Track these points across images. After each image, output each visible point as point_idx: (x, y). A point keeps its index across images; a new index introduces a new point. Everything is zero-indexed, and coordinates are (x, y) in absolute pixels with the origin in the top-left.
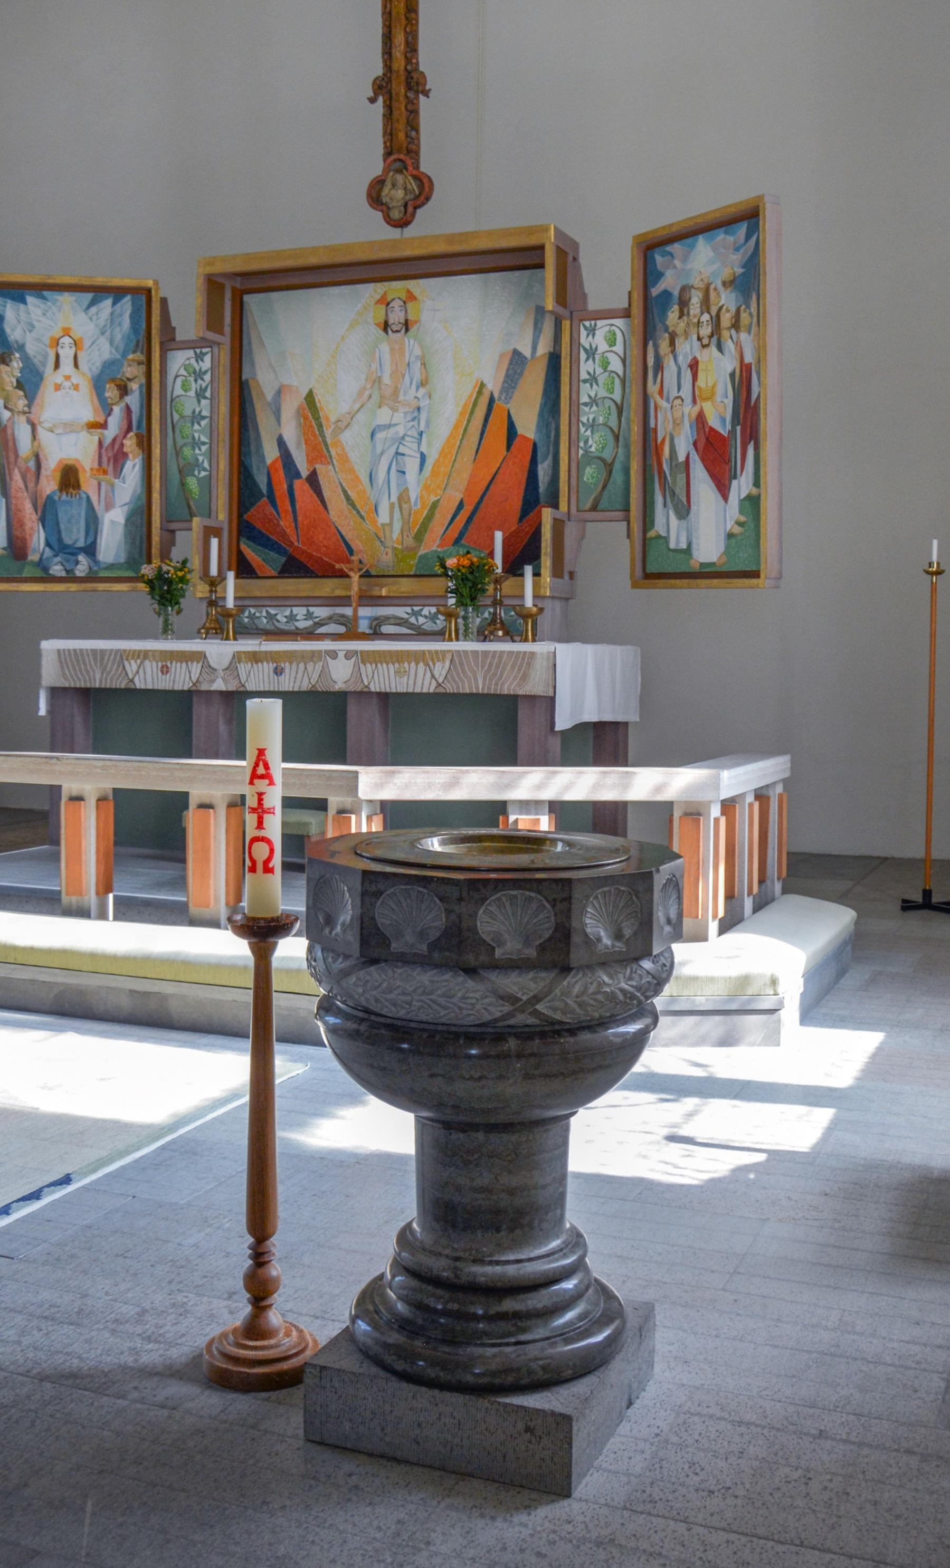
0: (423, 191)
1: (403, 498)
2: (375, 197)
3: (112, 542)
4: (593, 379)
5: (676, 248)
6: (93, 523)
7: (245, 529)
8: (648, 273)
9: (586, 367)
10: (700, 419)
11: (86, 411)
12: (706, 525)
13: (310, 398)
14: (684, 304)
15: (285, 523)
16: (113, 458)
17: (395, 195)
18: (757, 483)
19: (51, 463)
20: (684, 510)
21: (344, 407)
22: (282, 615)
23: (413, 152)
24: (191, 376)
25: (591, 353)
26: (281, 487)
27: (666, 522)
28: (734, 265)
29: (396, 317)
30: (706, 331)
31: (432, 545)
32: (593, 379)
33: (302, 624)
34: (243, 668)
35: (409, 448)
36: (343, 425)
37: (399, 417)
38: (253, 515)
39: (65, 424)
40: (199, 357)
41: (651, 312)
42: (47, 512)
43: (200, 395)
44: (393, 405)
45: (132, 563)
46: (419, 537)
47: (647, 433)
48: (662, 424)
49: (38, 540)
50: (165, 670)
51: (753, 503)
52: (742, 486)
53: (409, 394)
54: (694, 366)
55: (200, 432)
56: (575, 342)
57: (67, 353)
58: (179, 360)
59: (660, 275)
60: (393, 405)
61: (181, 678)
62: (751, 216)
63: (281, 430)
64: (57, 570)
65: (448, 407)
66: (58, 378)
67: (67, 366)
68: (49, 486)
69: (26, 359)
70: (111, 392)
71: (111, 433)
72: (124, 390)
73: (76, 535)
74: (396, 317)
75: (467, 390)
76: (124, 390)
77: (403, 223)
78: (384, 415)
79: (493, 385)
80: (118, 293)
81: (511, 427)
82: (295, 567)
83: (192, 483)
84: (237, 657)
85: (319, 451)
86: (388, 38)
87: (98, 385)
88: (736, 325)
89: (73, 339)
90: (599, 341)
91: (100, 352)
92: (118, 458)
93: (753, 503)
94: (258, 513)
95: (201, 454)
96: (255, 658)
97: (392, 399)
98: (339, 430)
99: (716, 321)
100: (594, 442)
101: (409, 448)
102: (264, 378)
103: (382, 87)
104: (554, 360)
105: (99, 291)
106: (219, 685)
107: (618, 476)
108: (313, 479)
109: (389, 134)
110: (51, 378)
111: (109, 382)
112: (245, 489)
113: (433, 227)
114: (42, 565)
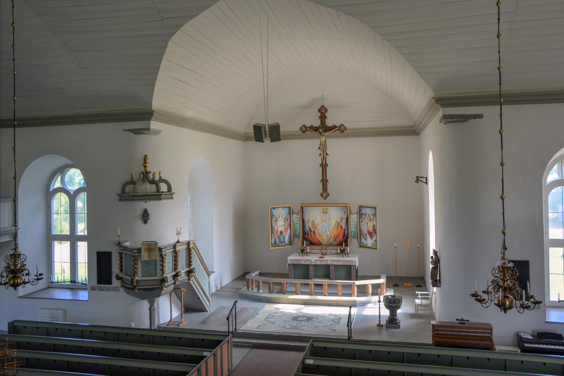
0: (328, 195)
1: (327, 235)
2: (322, 195)
3: (287, 241)
6: (284, 238)
7: (304, 238)
8: (360, 210)
9: (352, 220)
10: (368, 230)
11: (283, 224)
12: (369, 242)
13: (313, 221)
14: (365, 215)
15: (310, 237)
17: (324, 195)
20: (366, 240)
22: (313, 251)
23: (326, 190)
24: (296, 218)
27: (363, 240)
28: (373, 213)
29: (325, 211)
31: (331, 241)
35: (327, 228)
36: (318, 225)
38: (305, 236)
39: (280, 225)
41: (360, 215)
42: (279, 238)
44: (325, 223)
47: (360, 229)
48: (362, 228)
49: (278, 241)
51: (376, 241)
52: (374, 238)
55: (298, 225)
58: (294, 216)
60: (325, 223)
63: (309, 225)
65: (333, 223)
68: (279, 234)
73: (282, 240)
75: (335, 221)
77: (326, 198)
78: (324, 224)
79: (339, 221)
81: (341, 227)
82: (312, 244)
85: (315, 228)
86: (323, 174)
87: (284, 220)
89: (281, 213)
92: (287, 229)
93: (376, 241)
94: (306, 236)
95: (298, 228)
100: (353, 229)
103: (322, 181)
108: (314, 232)
109: (323, 187)
110: (279, 219)
111: (286, 219)
112: (304, 233)
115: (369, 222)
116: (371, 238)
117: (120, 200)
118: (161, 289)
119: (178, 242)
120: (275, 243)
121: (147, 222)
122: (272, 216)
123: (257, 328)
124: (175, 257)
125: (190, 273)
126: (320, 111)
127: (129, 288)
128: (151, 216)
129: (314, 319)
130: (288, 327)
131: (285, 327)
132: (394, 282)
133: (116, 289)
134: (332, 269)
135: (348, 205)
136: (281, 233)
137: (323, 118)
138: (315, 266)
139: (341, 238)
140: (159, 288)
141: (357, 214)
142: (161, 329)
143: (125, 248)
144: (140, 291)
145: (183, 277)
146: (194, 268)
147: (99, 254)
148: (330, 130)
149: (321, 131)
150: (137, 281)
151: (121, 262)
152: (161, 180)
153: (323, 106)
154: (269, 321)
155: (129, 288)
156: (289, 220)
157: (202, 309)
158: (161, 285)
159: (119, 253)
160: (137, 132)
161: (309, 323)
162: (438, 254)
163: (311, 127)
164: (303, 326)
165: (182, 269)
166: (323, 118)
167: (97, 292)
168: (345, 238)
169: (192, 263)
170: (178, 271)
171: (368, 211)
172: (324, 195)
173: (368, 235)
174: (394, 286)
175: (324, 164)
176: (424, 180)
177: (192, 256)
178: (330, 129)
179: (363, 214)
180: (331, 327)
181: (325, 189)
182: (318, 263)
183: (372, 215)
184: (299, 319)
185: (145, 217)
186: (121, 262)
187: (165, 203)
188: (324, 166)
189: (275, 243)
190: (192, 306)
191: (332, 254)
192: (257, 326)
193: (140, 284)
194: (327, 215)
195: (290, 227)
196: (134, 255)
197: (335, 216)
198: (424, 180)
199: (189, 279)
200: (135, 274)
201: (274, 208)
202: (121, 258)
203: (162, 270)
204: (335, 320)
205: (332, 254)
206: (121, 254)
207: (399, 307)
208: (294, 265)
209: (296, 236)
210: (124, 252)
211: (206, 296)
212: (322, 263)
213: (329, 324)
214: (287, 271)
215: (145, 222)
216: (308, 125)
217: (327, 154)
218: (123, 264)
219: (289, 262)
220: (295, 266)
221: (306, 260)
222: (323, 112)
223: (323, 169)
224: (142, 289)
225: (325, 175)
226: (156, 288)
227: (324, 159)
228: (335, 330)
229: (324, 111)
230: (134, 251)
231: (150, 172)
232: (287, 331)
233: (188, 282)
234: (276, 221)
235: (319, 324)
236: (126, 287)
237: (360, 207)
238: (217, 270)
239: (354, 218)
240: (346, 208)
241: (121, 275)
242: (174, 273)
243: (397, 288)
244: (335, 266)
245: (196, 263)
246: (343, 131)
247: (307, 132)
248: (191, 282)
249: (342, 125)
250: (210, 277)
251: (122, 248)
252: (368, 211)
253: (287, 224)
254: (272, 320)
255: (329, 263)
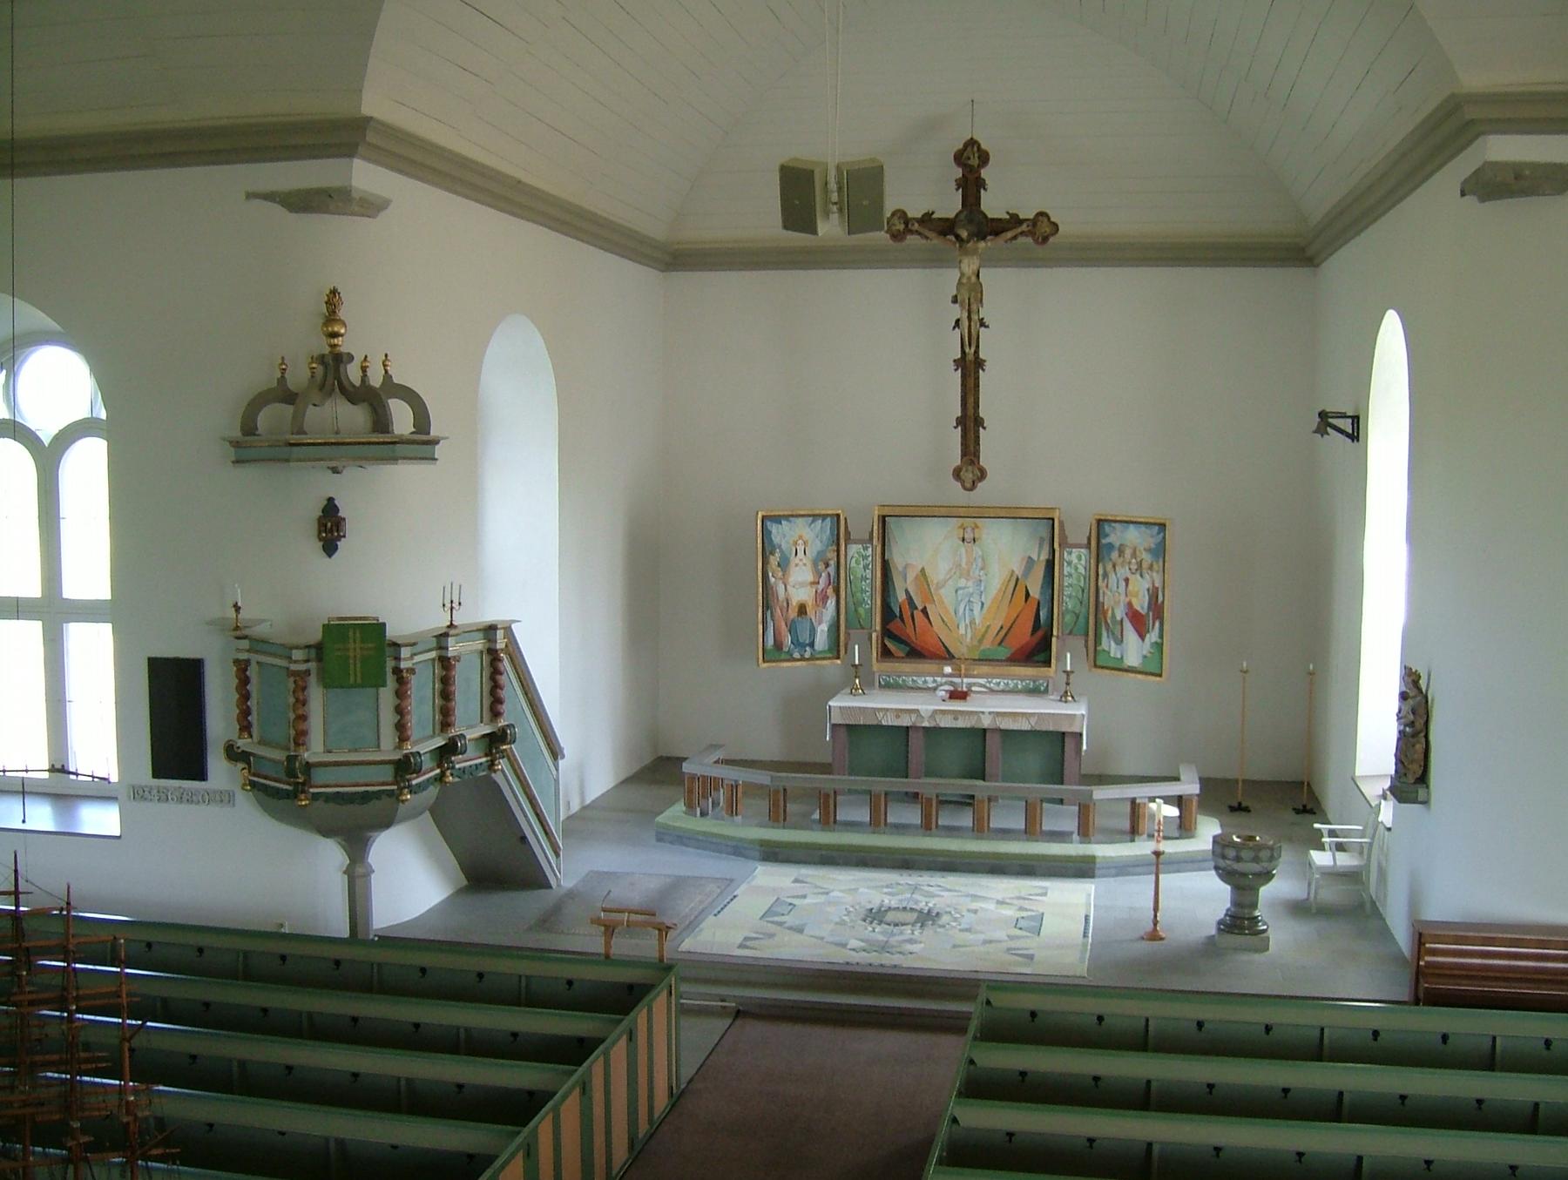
0: (983, 474)
1: (972, 622)
2: (957, 474)
3: (821, 641)
4: (1070, 575)
5: (1117, 525)
7: (886, 633)
9: (1067, 570)
10: (1130, 605)
11: (810, 578)
15: (910, 630)
16: (822, 598)
17: (968, 476)
18: (1161, 636)
19: (794, 602)
20: (1120, 641)
21: (941, 577)
22: (920, 681)
23: (977, 454)
25: (1069, 563)
26: (907, 615)
27: (1107, 643)
28: (1152, 542)
29: (969, 536)
30: (1134, 567)
31: (986, 645)
32: (1070, 575)
33: (931, 685)
34: (938, 718)
35: (975, 599)
36: (940, 586)
37: (970, 584)
39: (799, 584)
40: (865, 549)
41: (1100, 550)
42: (792, 629)
43: (866, 567)
44: (966, 577)
45: (830, 650)
46: (980, 641)
48: (1107, 600)
49: (788, 640)
50: (898, 717)
51: (1159, 646)
52: (1153, 636)
53: (976, 573)
54: (1127, 580)
55: (865, 585)
56: (1061, 556)
57: (801, 549)
58: (854, 549)
59: (1107, 536)
60: (966, 577)
61: (905, 721)
62: (1162, 526)
64: (796, 655)
65: (996, 581)
66: (797, 560)
67: (801, 553)
68: (793, 614)
69: (782, 552)
70: (821, 566)
71: (820, 587)
72: (827, 565)
74: (969, 536)
75: (1006, 574)
76: (827, 565)
78: (962, 583)
79: (1019, 572)
80: (824, 517)
82: (915, 653)
83: (861, 611)
84: (935, 711)
85: (928, 596)
87: (815, 564)
88: (1151, 567)
90: (1074, 558)
91: (816, 547)
92: (825, 598)
93: (1159, 646)
95: (866, 596)
96: (943, 712)
97: (967, 576)
98: (939, 587)
99: (1140, 564)
101: (975, 599)
102: (898, 559)
103: (961, 421)
104: (1050, 565)
105: (815, 517)
106: (926, 724)
107: (1082, 620)
108: (924, 611)
109: (964, 444)
110: (794, 560)
111: (820, 561)
112: (888, 613)
113: (986, 493)
114: (790, 653)
115: (1135, 580)
116: (1142, 637)
117: (237, 462)
118: (395, 796)
119: (451, 626)
120: (778, 645)
121: (336, 548)
122: (768, 548)
123: (741, 946)
124: (446, 681)
125: (496, 741)
126: (959, 158)
127: (276, 794)
128: (349, 527)
129: (945, 919)
130: (854, 943)
131: (844, 945)
132: (1226, 796)
133: (226, 798)
134: (993, 743)
135: (1056, 515)
136: (802, 609)
137: (971, 185)
138: (933, 733)
139: (1024, 635)
140: (390, 794)
141: (1088, 546)
142: (388, 941)
143: (259, 644)
144: (319, 804)
145: (470, 759)
146: (511, 726)
147: (158, 667)
148: (997, 234)
149: (964, 234)
150: (308, 767)
151: (245, 696)
152: (392, 388)
153: (972, 143)
154: (781, 924)
155: (276, 794)
156: (833, 563)
157: (532, 878)
158: (396, 782)
159: (236, 662)
160: (304, 202)
161: (929, 931)
162: (1423, 683)
163: (927, 219)
164: (911, 941)
165: (471, 726)
166: (971, 185)
167: (153, 808)
168: (1040, 633)
169: (505, 708)
170: (453, 732)
171: (1133, 537)
172: (968, 476)
173: (1128, 626)
174: (1232, 809)
175: (970, 357)
176: (1346, 425)
177: (503, 679)
178: (995, 228)
179: (1111, 546)
180: (1013, 944)
181: (970, 449)
182: (946, 722)
183: (1149, 550)
184: (890, 917)
185: (330, 528)
186: (245, 696)
187: (405, 475)
188: (970, 367)
189: (778, 645)
190: (495, 862)
191: (992, 691)
192: (739, 940)
193: (319, 776)
194: (977, 550)
195: (837, 591)
196: (293, 667)
197: (1006, 552)
198: (1346, 425)
199: (491, 765)
200: (300, 738)
201: (777, 519)
202: (244, 681)
203: (401, 728)
204: (1022, 923)
205: (992, 691)
206: (242, 667)
207: (1267, 876)
208: (849, 727)
209: (855, 623)
210: (255, 658)
211: (547, 832)
212: (961, 724)
213: (1000, 934)
214: (825, 757)
215: (330, 548)
216: (915, 212)
217: (982, 324)
218: (253, 703)
219: (837, 719)
220: (856, 732)
221: (899, 713)
222: (971, 164)
223: (964, 377)
224: (328, 798)
225: (971, 400)
226: (377, 795)
227: (971, 341)
228: (1031, 957)
229: (975, 162)
230: (298, 655)
231: (351, 358)
232: (856, 958)
233: (488, 778)
234: (784, 565)
235: (970, 936)
236: (265, 789)
237: (1099, 521)
238: (581, 732)
239: (1075, 562)
240: (1050, 528)
241: (243, 744)
242: (440, 742)
243: (1240, 818)
244: (1007, 734)
245: (514, 708)
246: (1045, 239)
247: (912, 240)
248: (498, 777)
249: (1042, 214)
250: (561, 762)
251: (245, 644)
252: (1133, 536)
253: (823, 581)
254: (789, 920)
255: (986, 722)
